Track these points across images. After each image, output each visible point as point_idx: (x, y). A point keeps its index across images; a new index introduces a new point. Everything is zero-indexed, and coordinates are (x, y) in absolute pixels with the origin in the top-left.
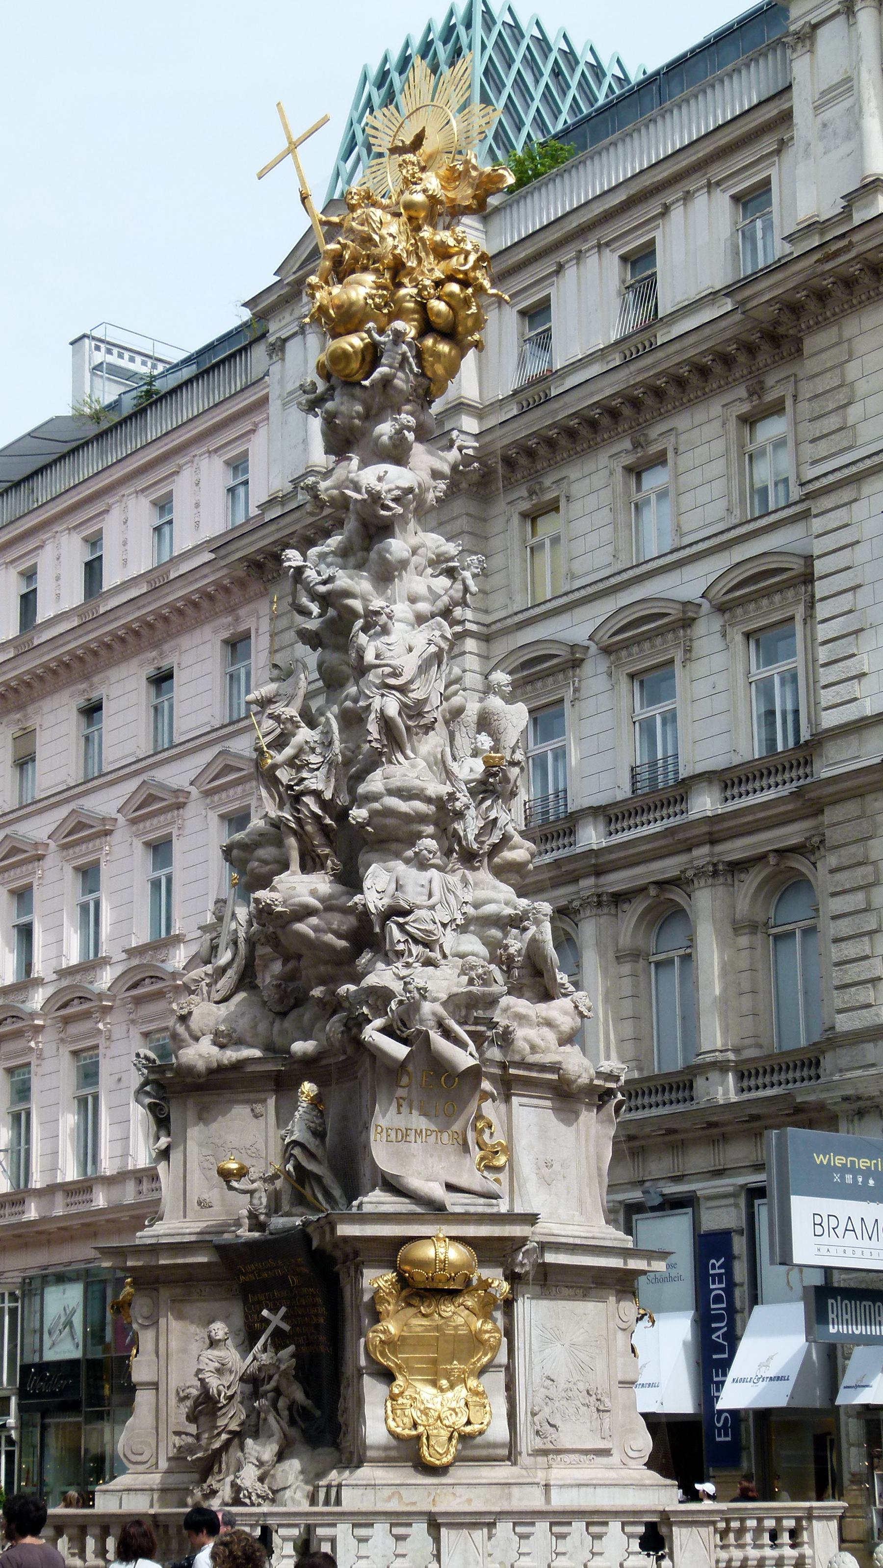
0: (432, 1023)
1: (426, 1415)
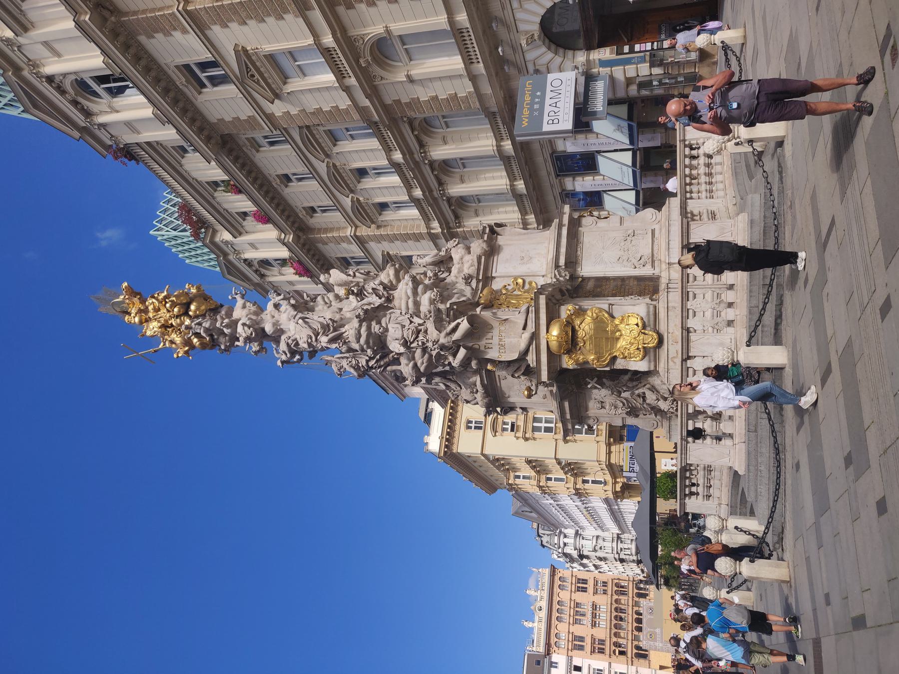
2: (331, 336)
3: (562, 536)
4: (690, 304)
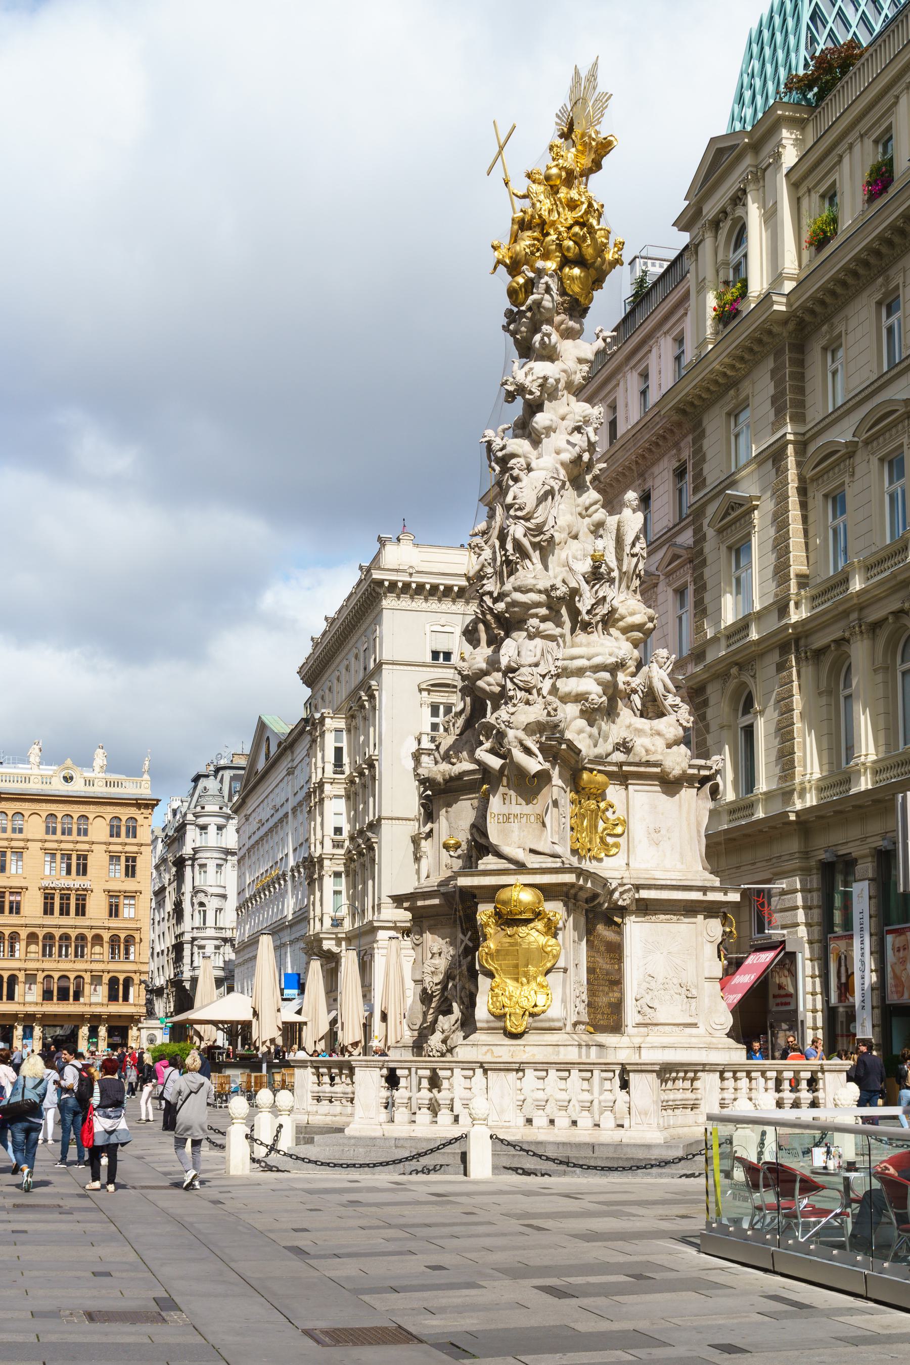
0: (516, 744)
1: (510, 1000)
2: (526, 542)
3: (221, 821)
4: (553, 1073)
